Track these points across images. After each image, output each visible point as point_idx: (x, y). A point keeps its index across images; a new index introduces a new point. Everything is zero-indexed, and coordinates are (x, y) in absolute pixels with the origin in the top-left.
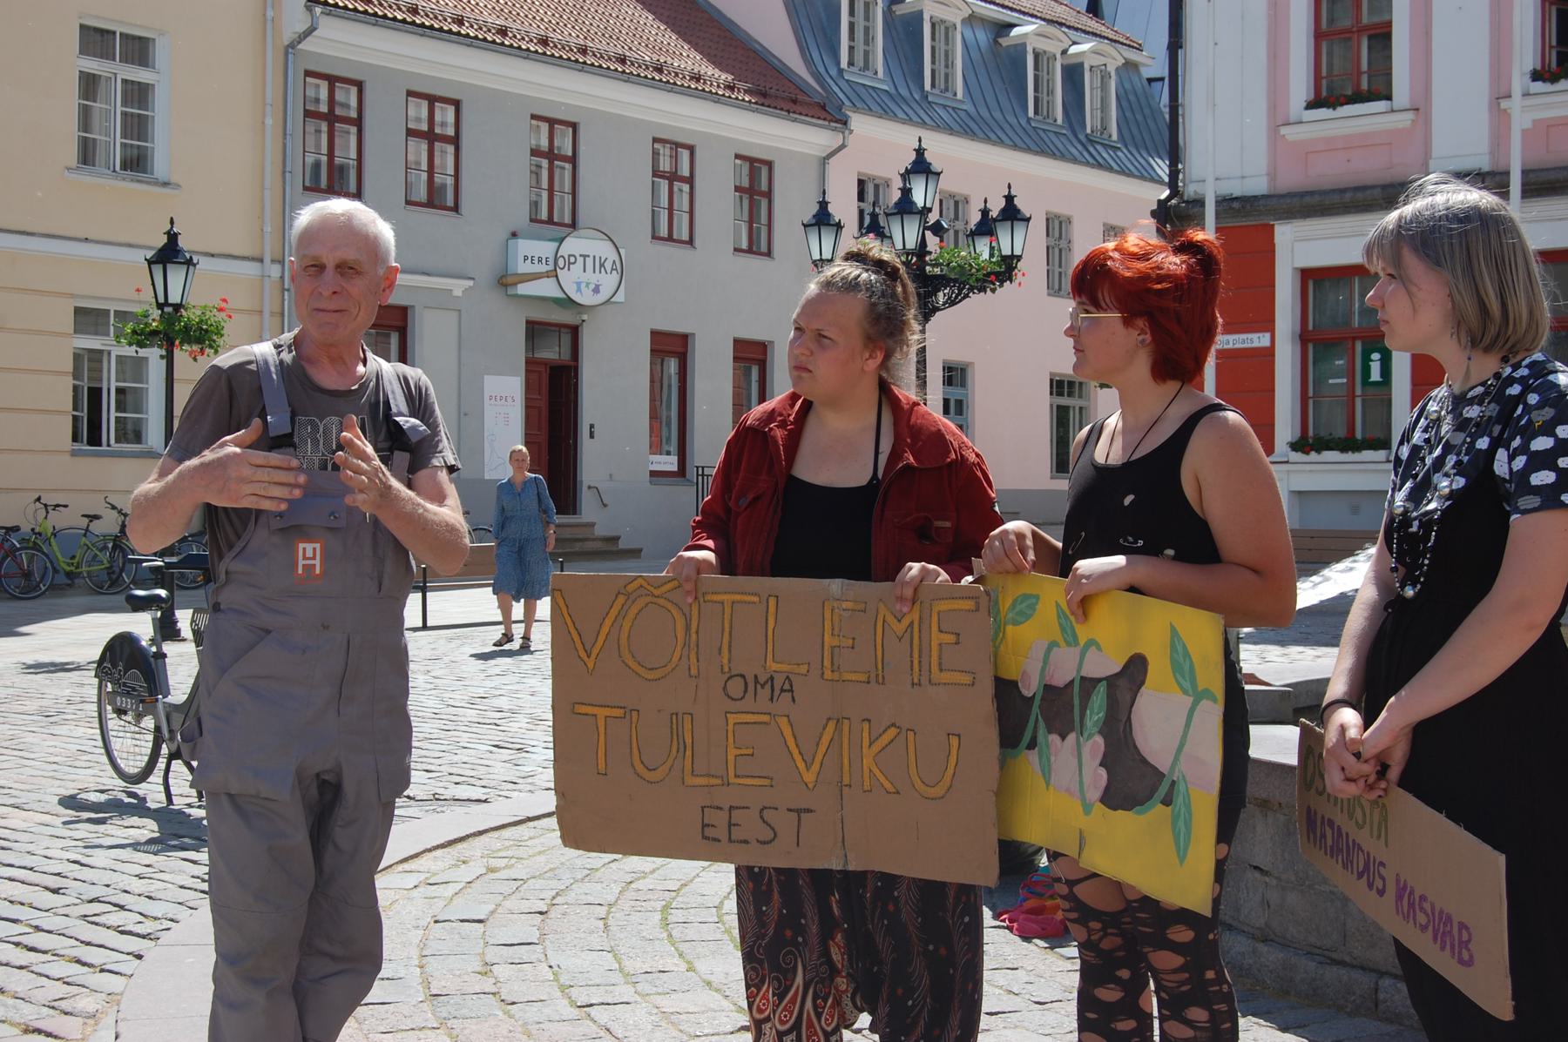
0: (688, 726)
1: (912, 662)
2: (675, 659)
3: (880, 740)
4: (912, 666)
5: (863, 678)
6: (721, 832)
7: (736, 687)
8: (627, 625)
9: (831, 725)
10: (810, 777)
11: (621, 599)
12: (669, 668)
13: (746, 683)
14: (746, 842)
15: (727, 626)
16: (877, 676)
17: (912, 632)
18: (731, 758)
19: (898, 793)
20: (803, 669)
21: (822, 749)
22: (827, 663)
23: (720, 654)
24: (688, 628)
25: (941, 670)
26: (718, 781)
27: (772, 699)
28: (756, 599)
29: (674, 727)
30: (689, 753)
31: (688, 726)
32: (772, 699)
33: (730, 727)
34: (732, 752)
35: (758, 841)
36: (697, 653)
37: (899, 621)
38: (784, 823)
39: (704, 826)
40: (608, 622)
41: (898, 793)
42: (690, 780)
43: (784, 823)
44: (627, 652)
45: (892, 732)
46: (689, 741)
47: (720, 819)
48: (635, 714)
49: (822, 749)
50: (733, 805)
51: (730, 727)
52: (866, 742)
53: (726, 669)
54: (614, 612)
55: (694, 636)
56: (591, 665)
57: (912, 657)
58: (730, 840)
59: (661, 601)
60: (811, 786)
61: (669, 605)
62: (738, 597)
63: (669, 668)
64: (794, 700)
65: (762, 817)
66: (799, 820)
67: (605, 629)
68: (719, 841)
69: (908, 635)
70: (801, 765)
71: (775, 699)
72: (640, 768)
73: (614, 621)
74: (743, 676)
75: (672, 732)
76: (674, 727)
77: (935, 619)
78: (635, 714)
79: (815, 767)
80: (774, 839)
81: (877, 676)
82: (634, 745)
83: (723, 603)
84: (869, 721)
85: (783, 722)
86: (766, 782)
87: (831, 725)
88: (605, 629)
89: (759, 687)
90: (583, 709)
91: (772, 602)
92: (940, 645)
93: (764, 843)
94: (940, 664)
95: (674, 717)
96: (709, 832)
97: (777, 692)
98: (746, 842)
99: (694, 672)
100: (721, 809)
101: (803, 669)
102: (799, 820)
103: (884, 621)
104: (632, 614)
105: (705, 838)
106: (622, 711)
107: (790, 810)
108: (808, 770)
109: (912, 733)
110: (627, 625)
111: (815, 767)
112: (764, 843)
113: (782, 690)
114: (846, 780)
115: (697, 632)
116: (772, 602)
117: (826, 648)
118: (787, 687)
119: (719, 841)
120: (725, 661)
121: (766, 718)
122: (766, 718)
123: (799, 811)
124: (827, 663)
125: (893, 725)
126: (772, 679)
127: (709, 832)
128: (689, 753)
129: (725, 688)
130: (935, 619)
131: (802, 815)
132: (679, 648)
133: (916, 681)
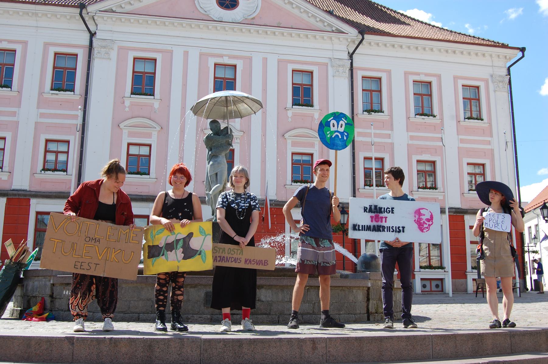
6: (79, 267)
7: (88, 239)
14: (84, 269)
15: (88, 228)
18: (84, 253)
24: (79, 227)
30: (75, 251)
34: (84, 251)
38: (93, 266)
39: (75, 265)
42: (74, 256)
43: (93, 266)
46: (75, 248)
47: (79, 264)
54: (64, 222)
55: (80, 229)
74: (89, 237)
90: (52, 239)
96: (76, 266)
98: (84, 269)
100: (79, 262)
104: (68, 223)
105: (75, 268)
120: (86, 234)
127: (76, 266)
128: (75, 251)
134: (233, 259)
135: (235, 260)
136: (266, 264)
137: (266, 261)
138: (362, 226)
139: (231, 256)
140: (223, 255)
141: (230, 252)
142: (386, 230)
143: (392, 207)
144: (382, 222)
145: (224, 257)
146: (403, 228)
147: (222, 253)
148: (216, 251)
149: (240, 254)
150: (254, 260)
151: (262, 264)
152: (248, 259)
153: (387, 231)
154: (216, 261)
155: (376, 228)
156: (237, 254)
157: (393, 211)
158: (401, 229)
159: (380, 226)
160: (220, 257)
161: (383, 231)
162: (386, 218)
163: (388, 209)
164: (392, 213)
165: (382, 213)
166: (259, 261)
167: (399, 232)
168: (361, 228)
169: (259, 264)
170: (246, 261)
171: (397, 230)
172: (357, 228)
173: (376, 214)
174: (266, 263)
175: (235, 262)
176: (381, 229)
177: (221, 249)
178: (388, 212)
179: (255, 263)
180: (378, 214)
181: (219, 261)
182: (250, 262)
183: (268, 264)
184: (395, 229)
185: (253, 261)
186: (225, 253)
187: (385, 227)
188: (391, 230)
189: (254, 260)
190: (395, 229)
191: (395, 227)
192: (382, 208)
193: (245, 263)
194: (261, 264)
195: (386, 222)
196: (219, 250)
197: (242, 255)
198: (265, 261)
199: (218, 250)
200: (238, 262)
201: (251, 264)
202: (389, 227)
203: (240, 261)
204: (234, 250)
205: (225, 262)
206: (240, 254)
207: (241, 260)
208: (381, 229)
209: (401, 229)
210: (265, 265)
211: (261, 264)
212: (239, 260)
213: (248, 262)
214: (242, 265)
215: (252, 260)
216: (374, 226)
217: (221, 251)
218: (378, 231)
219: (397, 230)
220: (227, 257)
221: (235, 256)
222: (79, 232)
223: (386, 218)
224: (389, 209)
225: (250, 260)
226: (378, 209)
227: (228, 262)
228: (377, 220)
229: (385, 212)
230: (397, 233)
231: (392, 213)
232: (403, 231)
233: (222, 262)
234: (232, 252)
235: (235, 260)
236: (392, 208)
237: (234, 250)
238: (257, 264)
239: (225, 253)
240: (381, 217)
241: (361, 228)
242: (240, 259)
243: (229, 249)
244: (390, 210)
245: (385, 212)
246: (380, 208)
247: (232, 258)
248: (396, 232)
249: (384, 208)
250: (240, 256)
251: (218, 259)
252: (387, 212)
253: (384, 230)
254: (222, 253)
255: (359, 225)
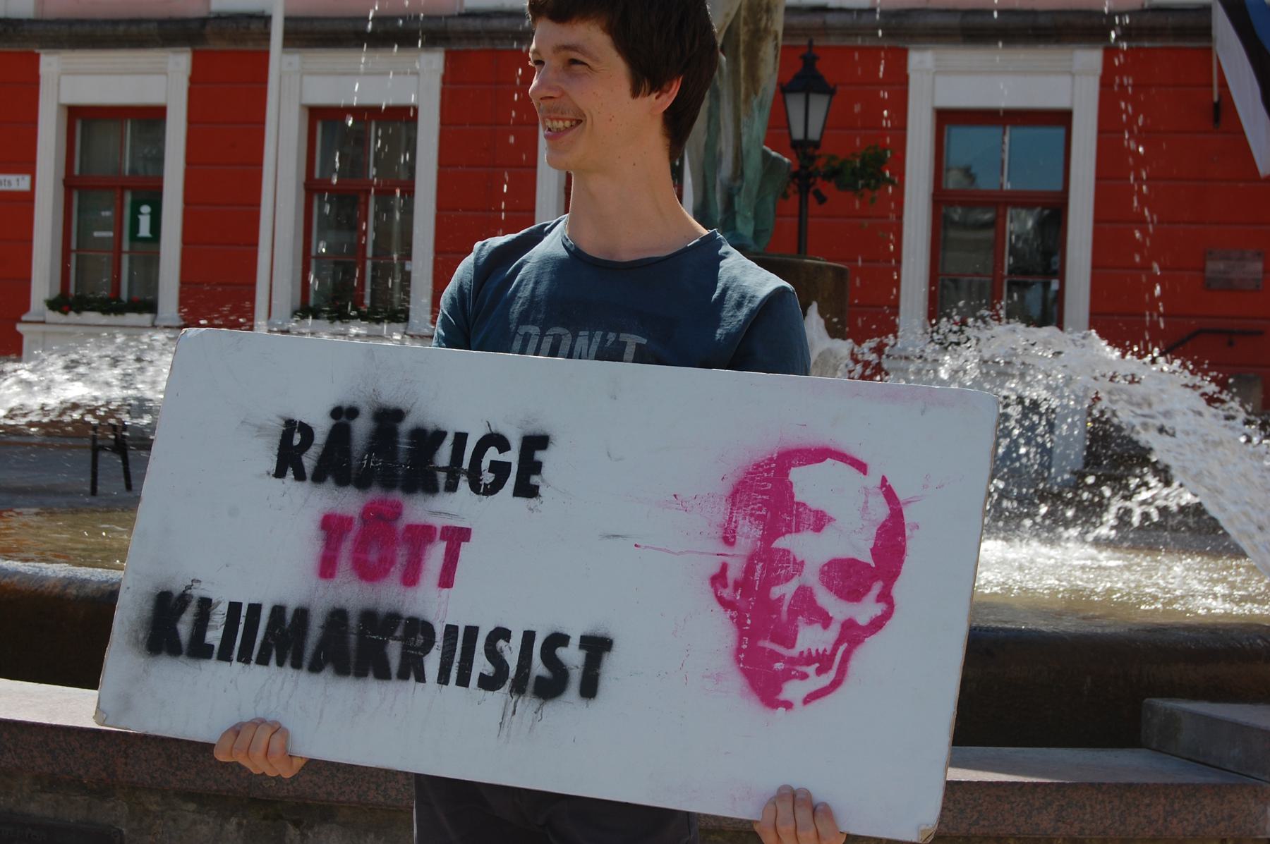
138: (234, 608)
142: (432, 662)
143: (535, 428)
144: (411, 578)
146: (597, 646)
153: (443, 678)
155: (353, 639)
157: (537, 468)
158: (572, 656)
159: (393, 618)
161: (403, 676)
162: (457, 536)
163: (492, 454)
164: (526, 490)
165: (432, 489)
167: (551, 688)
168: (214, 636)
171: (538, 668)
172: (184, 628)
173: (375, 493)
176: (394, 651)
178: (488, 478)
180: (397, 495)
184: (512, 658)
187: (428, 629)
188: (481, 665)
190: (512, 658)
191: (516, 640)
192: (440, 435)
195: (446, 580)
202: (472, 632)
208: (394, 651)
209: (572, 656)
216: (337, 617)
218: (361, 673)
219: (538, 668)
223: (457, 536)
224: (503, 444)
226: (403, 443)
228: (373, 556)
229: (464, 485)
230: (527, 704)
231: (526, 490)
232: (589, 689)
236: (535, 443)
240: (410, 528)
241: (214, 636)
244: (512, 457)
245: (464, 485)
246: (428, 440)
248: (519, 688)
249: (461, 439)
252: (475, 487)
253: (412, 669)
255: (206, 605)
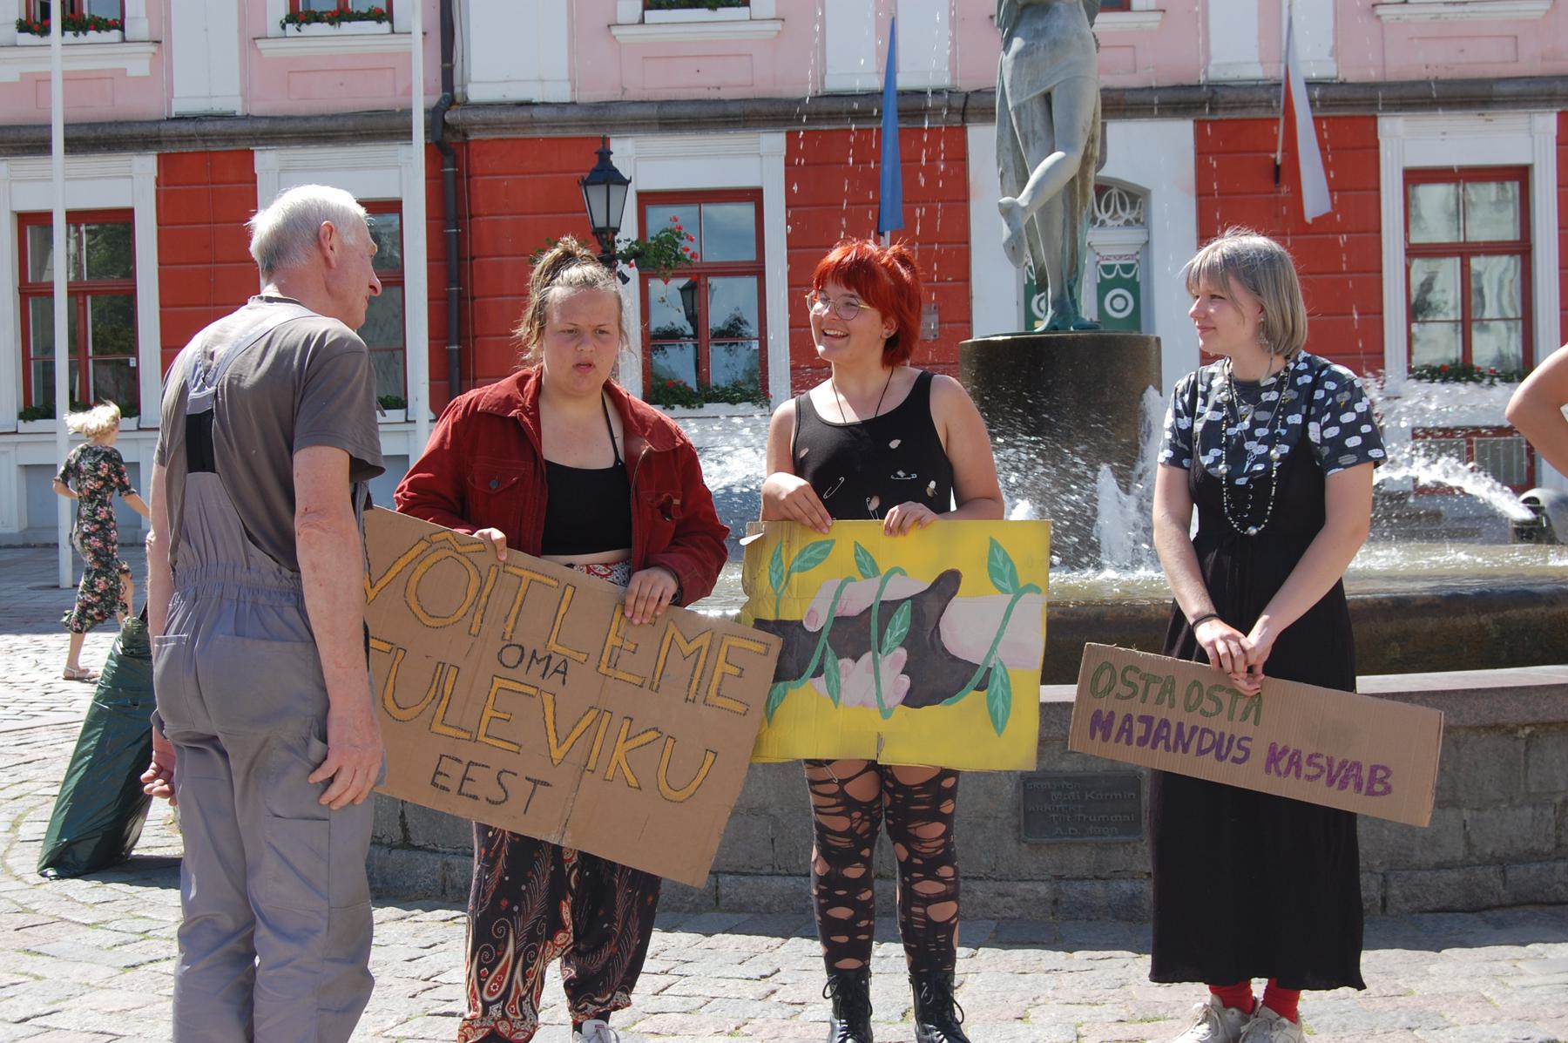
0: (451, 678)
1: (692, 680)
2: (461, 613)
3: (637, 739)
4: (691, 683)
5: (638, 681)
6: (453, 784)
7: (511, 656)
8: (421, 569)
9: (593, 714)
10: (557, 754)
11: (423, 545)
12: (451, 620)
13: (523, 655)
14: (475, 798)
16: (652, 683)
17: (698, 656)
18: (486, 718)
19: (640, 788)
20: (582, 657)
21: (577, 732)
22: (605, 658)
23: (505, 621)
24: (481, 589)
25: (718, 695)
26: (467, 736)
27: (543, 676)
28: (555, 583)
29: (438, 675)
30: (444, 702)
31: (451, 678)
32: (543, 676)
33: (494, 690)
34: (489, 713)
35: (487, 799)
36: (483, 615)
37: (688, 643)
39: (437, 773)
40: (402, 562)
41: (640, 788)
44: (413, 593)
45: (653, 735)
46: (448, 691)
47: (457, 771)
48: (401, 653)
49: (577, 732)
50: (474, 761)
51: (494, 690)
52: (622, 737)
53: (507, 637)
55: (484, 600)
56: (371, 597)
57: (693, 675)
58: (460, 792)
59: (462, 559)
60: (555, 762)
61: (468, 565)
62: (538, 577)
63: (451, 620)
64: (564, 682)
65: (498, 779)
66: (534, 790)
67: (397, 568)
68: (448, 790)
69: (695, 656)
70: (553, 742)
71: (547, 676)
72: (390, 704)
73: (410, 562)
74: (522, 648)
75: (434, 675)
76: (438, 675)
77: (724, 649)
78: (401, 653)
79: (565, 747)
80: (503, 802)
81: (652, 683)
82: (391, 682)
83: (521, 578)
84: (631, 720)
85: (548, 699)
86: (515, 748)
87: (593, 714)
88: (397, 568)
89: (534, 661)
91: (569, 591)
92: (724, 673)
93: (493, 803)
94: (719, 689)
95: (440, 666)
96: (440, 780)
97: (549, 672)
98: (475, 798)
99: (474, 630)
100: (460, 761)
101: (582, 657)
102: (534, 790)
103: (672, 638)
105: (434, 784)
106: (389, 647)
107: (528, 779)
108: (558, 747)
109: (672, 740)
110: (421, 569)
111: (565, 747)
112: (493, 803)
113: (556, 671)
114: (591, 766)
115: (488, 597)
116: (569, 591)
117: (607, 645)
118: (561, 668)
119: (448, 790)
120: (509, 629)
121: (532, 691)
122: (532, 691)
123: (536, 782)
124: (605, 658)
125: (656, 729)
126: (550, 657)
127: (440, 780)
128: (444, 702)
129: (500, 654)
130: (724, 649)
131: (538, 786)
132: (466, 606)
133: (690, 697)
134: (1208, 741)
135: (1220, 748)
136: (1378, 787)
137: (1380, 774)
139: (1202, 723)
140: (1161, 712)
141: (1199, 701)
145: (1165, 723)
147: (1159, 701)
148: (1129, 691)
149: (1245, 717)
150: (1318, 756)
151: (1358, 786)
152: (1285, 750)
154: (1129, 742)
156: (1230, 718)
160: (1147, 720)
166: (1343, 765)
169: (1343, 786)
170: (1274, 757)
174: (1382, 781)
175: (1220, 758)
177: (1156, 679)
179: (1318, 776)
181: (1142, 741)
182: (1295, 763)
183: (1388, 789)
185: (1310, 763)
186: (1172, 706)
189: (1318, 756)
193: (1268, 770)
194: (1352, 782)
196: (1146, 689)
197: (1256, 723)
198: (1374, 769)
199: (1141, 684)
200: (1235, 760)
201: (1298, 775)
203: (1240, 754)
204: (1217, 694)
205: (1167, 748)
206: (1245, 717)
207: (1247, 751)
210: (1370, 792)
211: (1352, 782)
212: (1239, 747)
213: (1283, 764)
214: (1250, 776)
215: (1304, 757)
217: (1155, 689)
220: (1180, 725)
221: (1219, 724)
222: (478, 617)
225: (1297, 753)
227: (1185, 750)
233: (1154, 746)
234: (1209, 705)
235: (1217, 745)
237: (1217, 694)
238: (1331, 782)
239: (1172, 706)
242: (1244, 743)
243: (1195, 683)
247: (1204, 731)
250: (1247, 728)
251: (1139, 730)
254: (1159, 701)
